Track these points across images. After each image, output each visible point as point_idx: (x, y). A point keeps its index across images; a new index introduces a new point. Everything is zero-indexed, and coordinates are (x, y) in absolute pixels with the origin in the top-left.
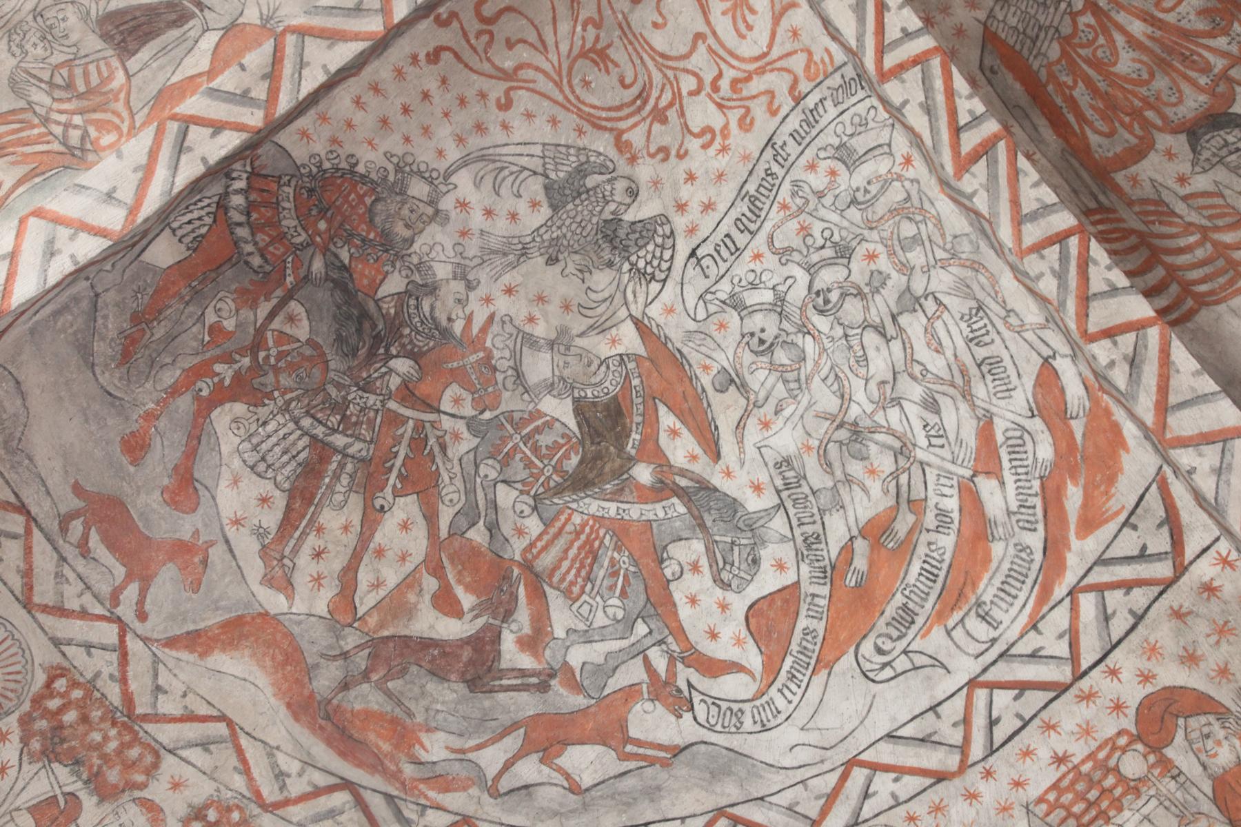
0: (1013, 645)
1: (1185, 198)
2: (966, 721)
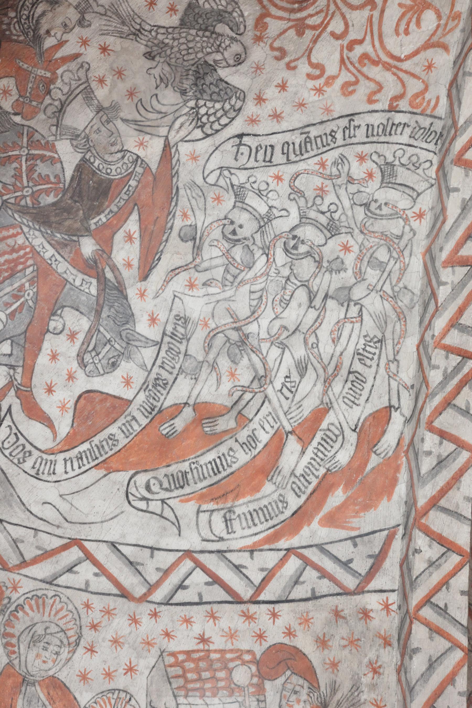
0: (231, 551)
2: (167, 573)
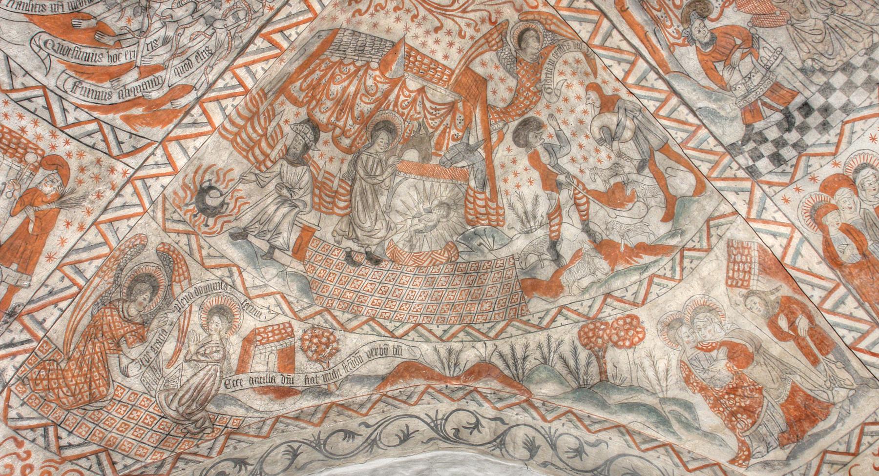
1: (278, 124)
2: (26, 88)
